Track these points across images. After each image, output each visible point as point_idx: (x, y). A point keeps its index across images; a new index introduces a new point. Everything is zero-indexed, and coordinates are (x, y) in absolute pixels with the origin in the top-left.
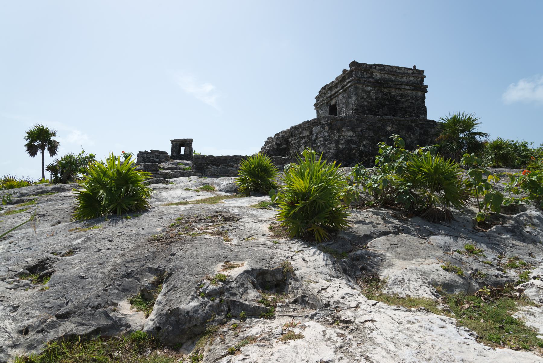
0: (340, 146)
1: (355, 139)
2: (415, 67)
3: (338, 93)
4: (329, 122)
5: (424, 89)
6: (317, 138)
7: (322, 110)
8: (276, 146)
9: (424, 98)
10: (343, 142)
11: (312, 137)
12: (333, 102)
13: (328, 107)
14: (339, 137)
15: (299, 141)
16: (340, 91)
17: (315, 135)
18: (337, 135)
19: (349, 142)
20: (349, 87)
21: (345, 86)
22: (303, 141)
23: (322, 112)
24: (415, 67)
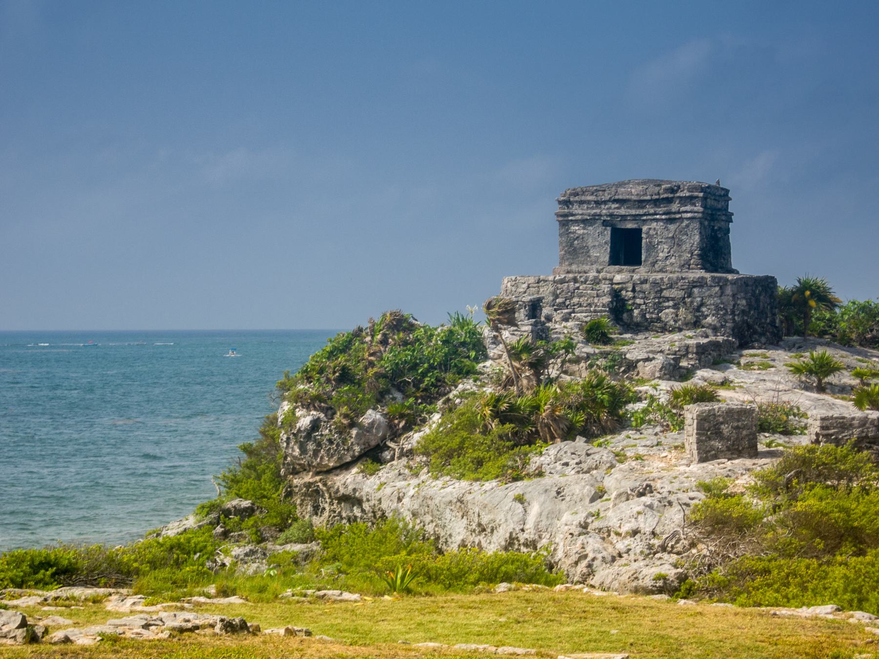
0: (736, 318)
1: (747, 309)
2: (718, 182)
3: (649, 217)
4: (721, 284)
5: (729, 218)
6: (702, 304)
7: (584, 228)
8: (611, 306)
9: (728, 230)
10: (737, 313)
11: (692, 302)
12: (630, 225)
13: (609, 228)
14: (734, 306)
15: (659, 303)
16: (658, 217)
17: (699, 299)
18: (732, 303)
19: (743, 312)
20: (687, 219)
21: (675, 213)
22: (671, 303)
23: (585, 231)
24: (718, 182)
